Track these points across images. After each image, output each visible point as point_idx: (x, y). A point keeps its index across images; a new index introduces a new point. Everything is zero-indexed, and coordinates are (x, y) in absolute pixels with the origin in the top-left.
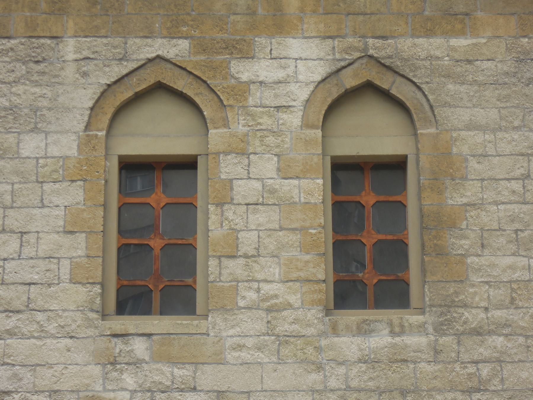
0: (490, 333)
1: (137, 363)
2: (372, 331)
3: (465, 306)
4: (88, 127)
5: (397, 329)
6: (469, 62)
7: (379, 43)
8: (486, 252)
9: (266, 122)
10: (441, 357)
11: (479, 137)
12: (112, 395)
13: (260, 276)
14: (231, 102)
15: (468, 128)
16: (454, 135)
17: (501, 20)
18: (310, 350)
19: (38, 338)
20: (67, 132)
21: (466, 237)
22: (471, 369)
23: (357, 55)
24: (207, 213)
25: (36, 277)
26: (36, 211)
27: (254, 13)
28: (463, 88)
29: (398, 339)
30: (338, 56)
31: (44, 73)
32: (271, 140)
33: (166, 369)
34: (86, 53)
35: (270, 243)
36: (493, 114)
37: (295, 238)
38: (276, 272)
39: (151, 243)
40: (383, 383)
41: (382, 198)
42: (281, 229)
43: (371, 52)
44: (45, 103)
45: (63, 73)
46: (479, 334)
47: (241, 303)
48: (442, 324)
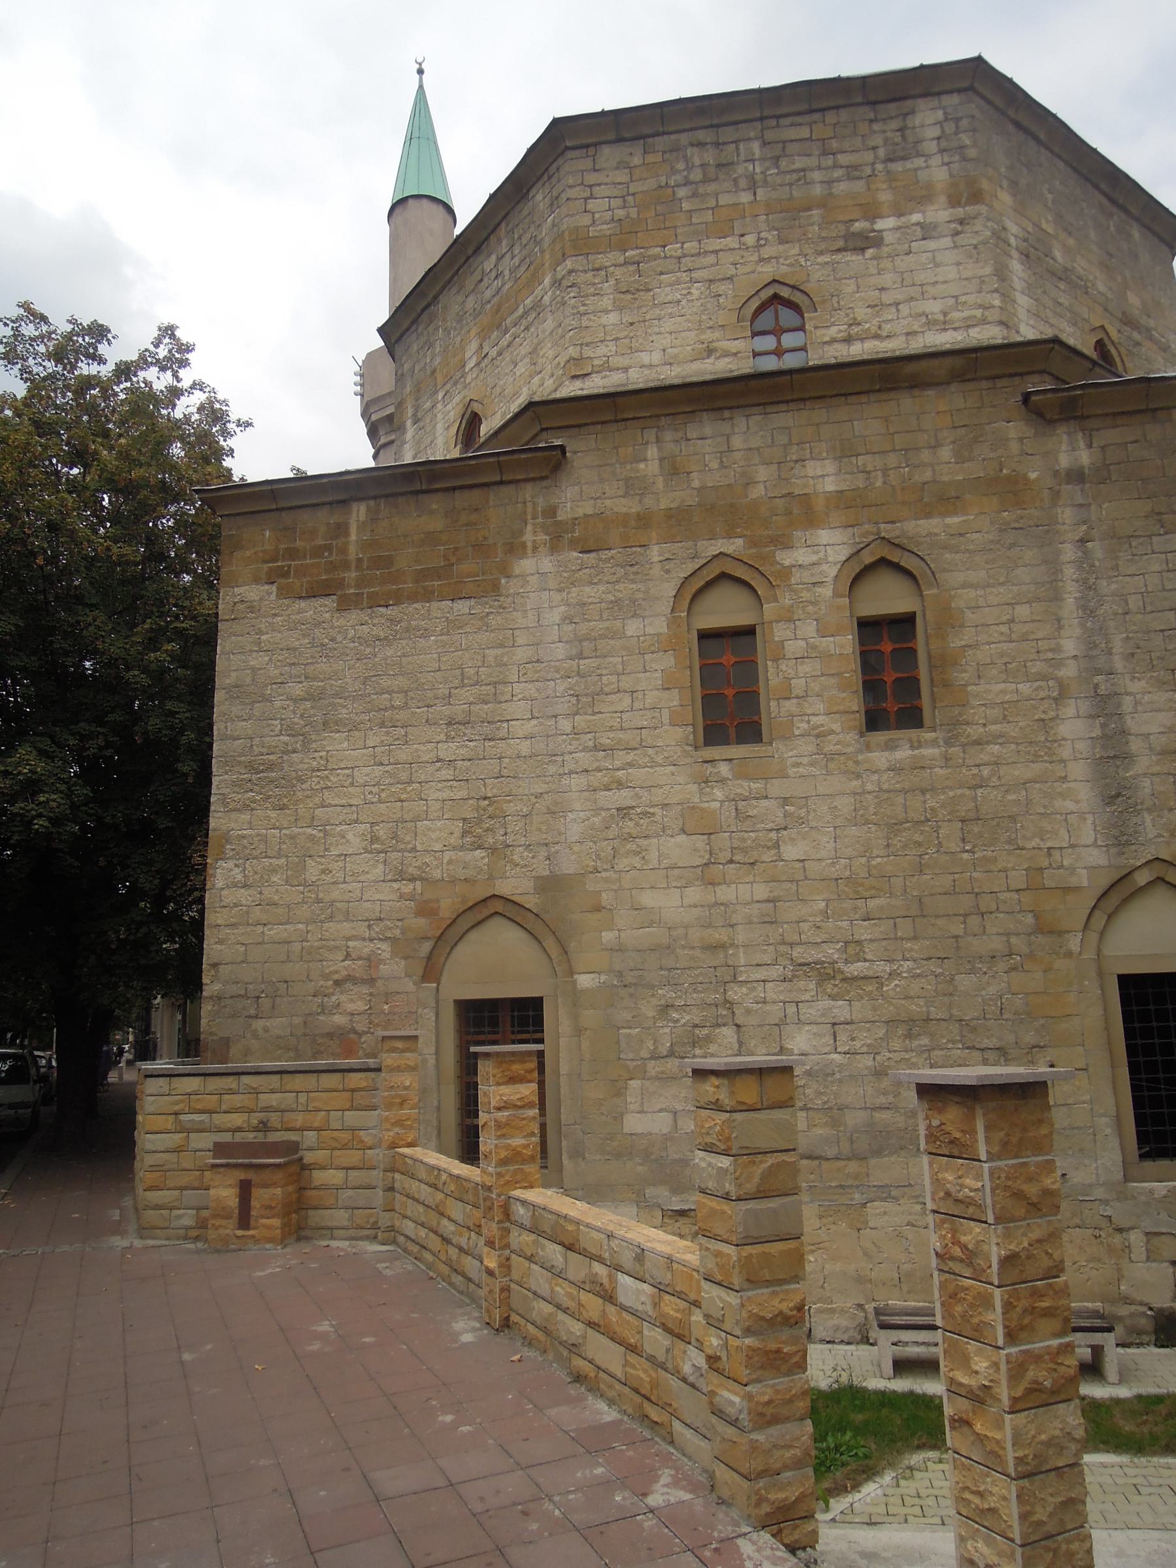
0: (988, 743)
1: (723, 781)
2: (897, 746)
3: (968, 724)
4: (673, 610)
5: (916, 744)
6: (961, 535)
7: (889, 526)
8: (982, 681)
9: (806, 595)
10: (951, 763)
11: (972, 593)
12: (707, 805)
13: (809, 712)
14: (778, 583)
15: (963, 587)
16: (953, 593)
18: (850, 763)
19: (651, 767)
20: (658, 615)
21: (965, 672)
22: (975, 771)
23: (872, 538)
24: (766, 666)
26: (641, 675)
27: (789, 513)
28: (958, 556)
29: (917, 752)
30: (857, 540)
31: (637, 573)
32: (810, 609)
33: (745, 784)
34: (667, 556)
36: (982, 574)
37: (833, 681)
38: (821, 707)
39: (726, 692)
41: (897, 646)
42: (823, 675)
43: (883, 534)
44: (641, 595)
45: (651, 572)
46: (979, 744)
47: (797, 732)
48: (950, 738)
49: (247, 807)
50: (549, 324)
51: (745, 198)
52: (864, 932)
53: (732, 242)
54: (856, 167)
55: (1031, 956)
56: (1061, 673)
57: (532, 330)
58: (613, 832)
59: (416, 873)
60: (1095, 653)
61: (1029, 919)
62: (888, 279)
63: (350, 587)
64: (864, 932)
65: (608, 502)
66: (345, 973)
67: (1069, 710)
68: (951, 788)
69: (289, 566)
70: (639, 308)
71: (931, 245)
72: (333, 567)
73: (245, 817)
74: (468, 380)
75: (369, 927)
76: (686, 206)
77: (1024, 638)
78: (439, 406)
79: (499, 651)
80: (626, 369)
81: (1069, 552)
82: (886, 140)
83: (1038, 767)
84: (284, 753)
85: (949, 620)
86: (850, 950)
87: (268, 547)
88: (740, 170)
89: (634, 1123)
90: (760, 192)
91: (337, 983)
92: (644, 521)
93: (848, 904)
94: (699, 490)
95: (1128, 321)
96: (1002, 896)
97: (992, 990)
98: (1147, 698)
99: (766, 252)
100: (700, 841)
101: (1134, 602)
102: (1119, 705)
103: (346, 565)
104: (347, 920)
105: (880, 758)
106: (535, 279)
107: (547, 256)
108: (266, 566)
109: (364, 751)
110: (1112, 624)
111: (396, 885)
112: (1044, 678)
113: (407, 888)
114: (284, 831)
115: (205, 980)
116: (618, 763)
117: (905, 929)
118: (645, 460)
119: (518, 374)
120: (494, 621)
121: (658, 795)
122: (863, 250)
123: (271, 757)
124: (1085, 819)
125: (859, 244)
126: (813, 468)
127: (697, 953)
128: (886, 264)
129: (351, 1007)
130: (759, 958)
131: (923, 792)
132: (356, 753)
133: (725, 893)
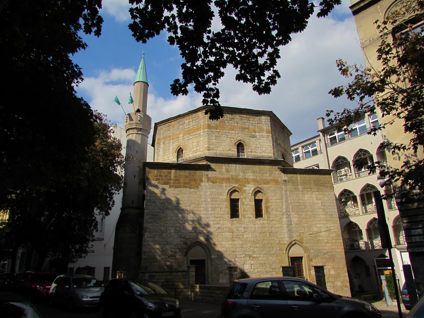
3: (270, 218)
4: (227, 195)
15: (270, 196)
17: (273, 183)
22: (271, 225)
25: (222, 214)
27: (245, 181)
33: (238, 225)
35: (249, 210)
36: (273, 194)
40: (262, 227)
49: (151, 223)
50: (202, 139)
51: (236, 125)
52: (256, 250)
53: (234, 132)
54: (253, 124)
55: (279, 254)
56: (283, 211)
57: (197, 138)
58: (217, 232)
59: (184, 237)
60: (287, 208)
61: (279, 248)
62: (257, 143)
63: (171, 183)
64: (256, 250)
65: (217, 175)
66: (170, 254)
67: (284, 216)
68: (268, 227)
69: (160, 178)
70: (219, 140)
71: (264, 139)
72: (168, 179)
73: (151, 224)
74: (180, 141)
75: (175, 246)
76: (227, 124)
77: (278, 205)
78: (171, 143)
79: (199, 199)
80: (216, 150)
81: (284, 193)
82: (257, 120)
83: (280, 225)
84: (159, 213)
85: (267, 201)
86: (254, 253)
87: (156, 174)
88: (235, 120)
89: (221, 281)
90: (238, 124)
91: (169, 256)
92: (223, 179)
93: (253, 245)
94: (231, 175)
95: (285, 150)
96: (275, 245)
97: (274, 259)
98: (294, 216)
99: (239, 135)
100: (231, 234)
101: (292, 201)
102: (291, 216)
103: (171, 179)
104: (171, 245)
105: (258, 222)
106: (199, 129)
107: (202, 126)
108: (155, 178)
109: (174, 214)
110: (290, 204)
111: (180, 239)
112: (280, 211)
113: (182, 239)
114: (159, 228)
115: (143, 255)
116: (218, 220)
117: (262, 249)
118: (223, 169)
119: (194, 145)
120: (197, 193)
121: (225, 226)
122: (254, 137)
123: (156, 214)
124: (286, 233)
125: (253, 137)
126: (248, 174)
127: (231, 252)
128: (257, 140)
129: (171, 261)
130: (240, 253)
131: (264, 228)
132: (172, 214)
133: (235, 243)
